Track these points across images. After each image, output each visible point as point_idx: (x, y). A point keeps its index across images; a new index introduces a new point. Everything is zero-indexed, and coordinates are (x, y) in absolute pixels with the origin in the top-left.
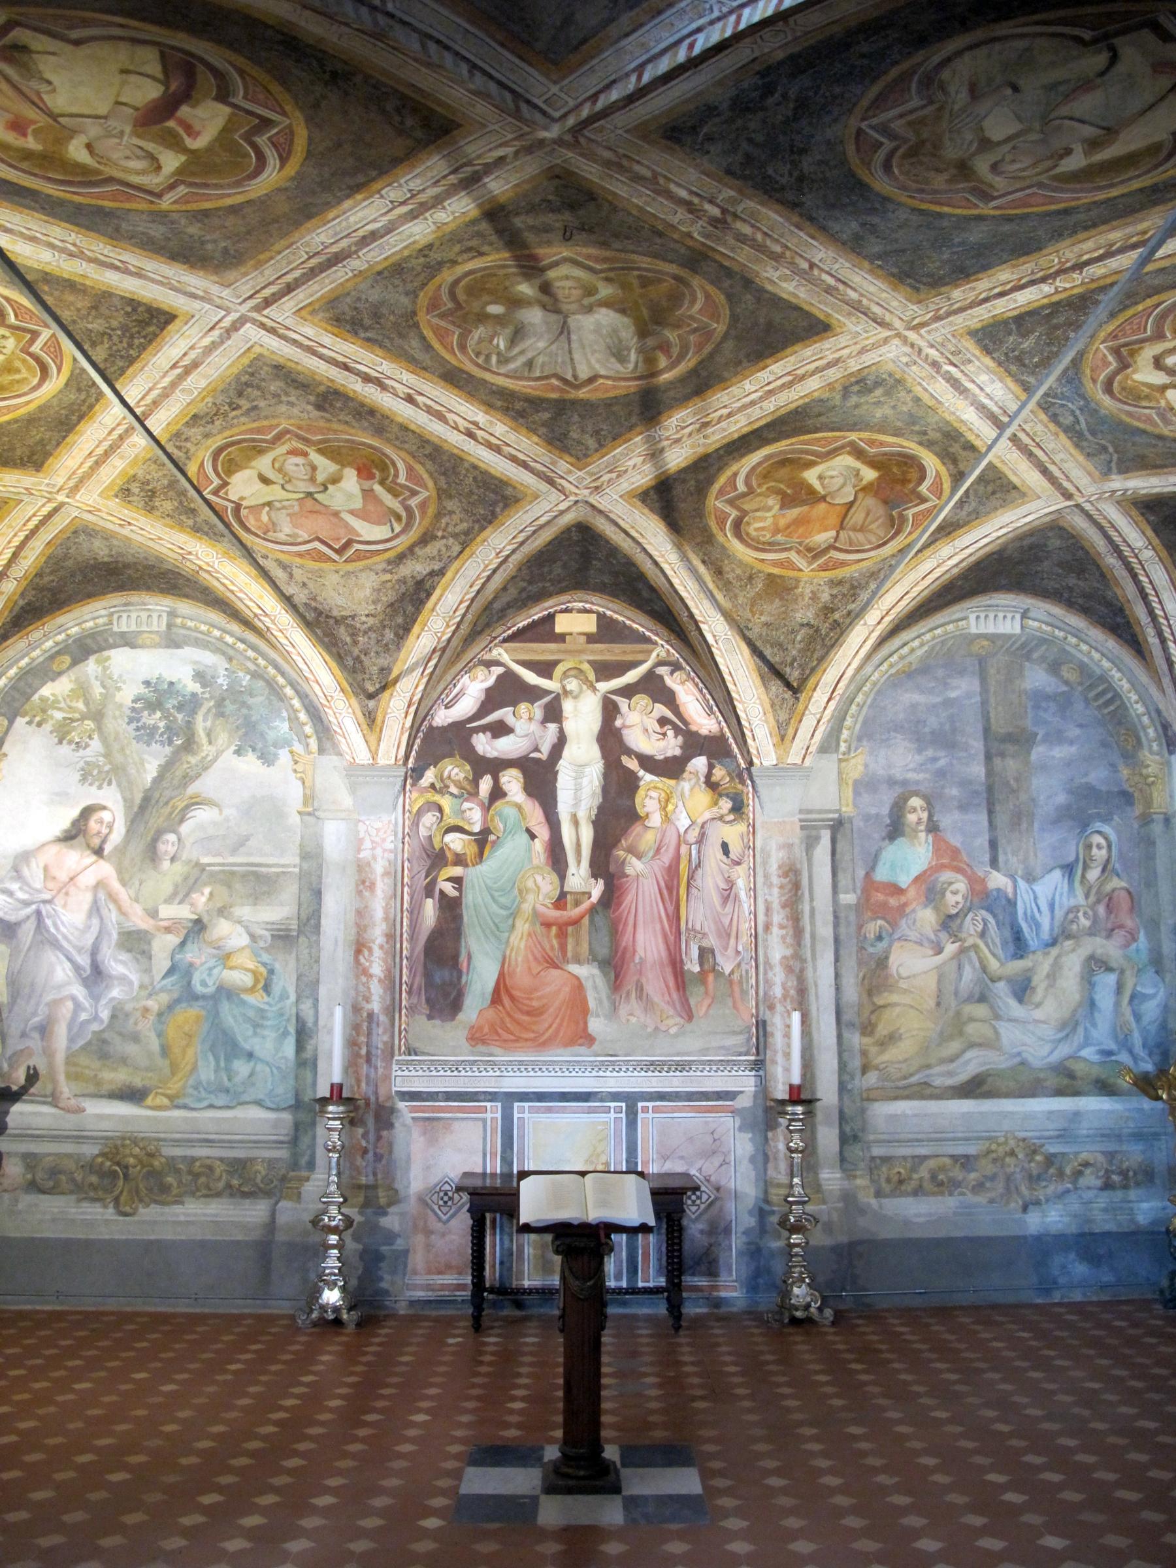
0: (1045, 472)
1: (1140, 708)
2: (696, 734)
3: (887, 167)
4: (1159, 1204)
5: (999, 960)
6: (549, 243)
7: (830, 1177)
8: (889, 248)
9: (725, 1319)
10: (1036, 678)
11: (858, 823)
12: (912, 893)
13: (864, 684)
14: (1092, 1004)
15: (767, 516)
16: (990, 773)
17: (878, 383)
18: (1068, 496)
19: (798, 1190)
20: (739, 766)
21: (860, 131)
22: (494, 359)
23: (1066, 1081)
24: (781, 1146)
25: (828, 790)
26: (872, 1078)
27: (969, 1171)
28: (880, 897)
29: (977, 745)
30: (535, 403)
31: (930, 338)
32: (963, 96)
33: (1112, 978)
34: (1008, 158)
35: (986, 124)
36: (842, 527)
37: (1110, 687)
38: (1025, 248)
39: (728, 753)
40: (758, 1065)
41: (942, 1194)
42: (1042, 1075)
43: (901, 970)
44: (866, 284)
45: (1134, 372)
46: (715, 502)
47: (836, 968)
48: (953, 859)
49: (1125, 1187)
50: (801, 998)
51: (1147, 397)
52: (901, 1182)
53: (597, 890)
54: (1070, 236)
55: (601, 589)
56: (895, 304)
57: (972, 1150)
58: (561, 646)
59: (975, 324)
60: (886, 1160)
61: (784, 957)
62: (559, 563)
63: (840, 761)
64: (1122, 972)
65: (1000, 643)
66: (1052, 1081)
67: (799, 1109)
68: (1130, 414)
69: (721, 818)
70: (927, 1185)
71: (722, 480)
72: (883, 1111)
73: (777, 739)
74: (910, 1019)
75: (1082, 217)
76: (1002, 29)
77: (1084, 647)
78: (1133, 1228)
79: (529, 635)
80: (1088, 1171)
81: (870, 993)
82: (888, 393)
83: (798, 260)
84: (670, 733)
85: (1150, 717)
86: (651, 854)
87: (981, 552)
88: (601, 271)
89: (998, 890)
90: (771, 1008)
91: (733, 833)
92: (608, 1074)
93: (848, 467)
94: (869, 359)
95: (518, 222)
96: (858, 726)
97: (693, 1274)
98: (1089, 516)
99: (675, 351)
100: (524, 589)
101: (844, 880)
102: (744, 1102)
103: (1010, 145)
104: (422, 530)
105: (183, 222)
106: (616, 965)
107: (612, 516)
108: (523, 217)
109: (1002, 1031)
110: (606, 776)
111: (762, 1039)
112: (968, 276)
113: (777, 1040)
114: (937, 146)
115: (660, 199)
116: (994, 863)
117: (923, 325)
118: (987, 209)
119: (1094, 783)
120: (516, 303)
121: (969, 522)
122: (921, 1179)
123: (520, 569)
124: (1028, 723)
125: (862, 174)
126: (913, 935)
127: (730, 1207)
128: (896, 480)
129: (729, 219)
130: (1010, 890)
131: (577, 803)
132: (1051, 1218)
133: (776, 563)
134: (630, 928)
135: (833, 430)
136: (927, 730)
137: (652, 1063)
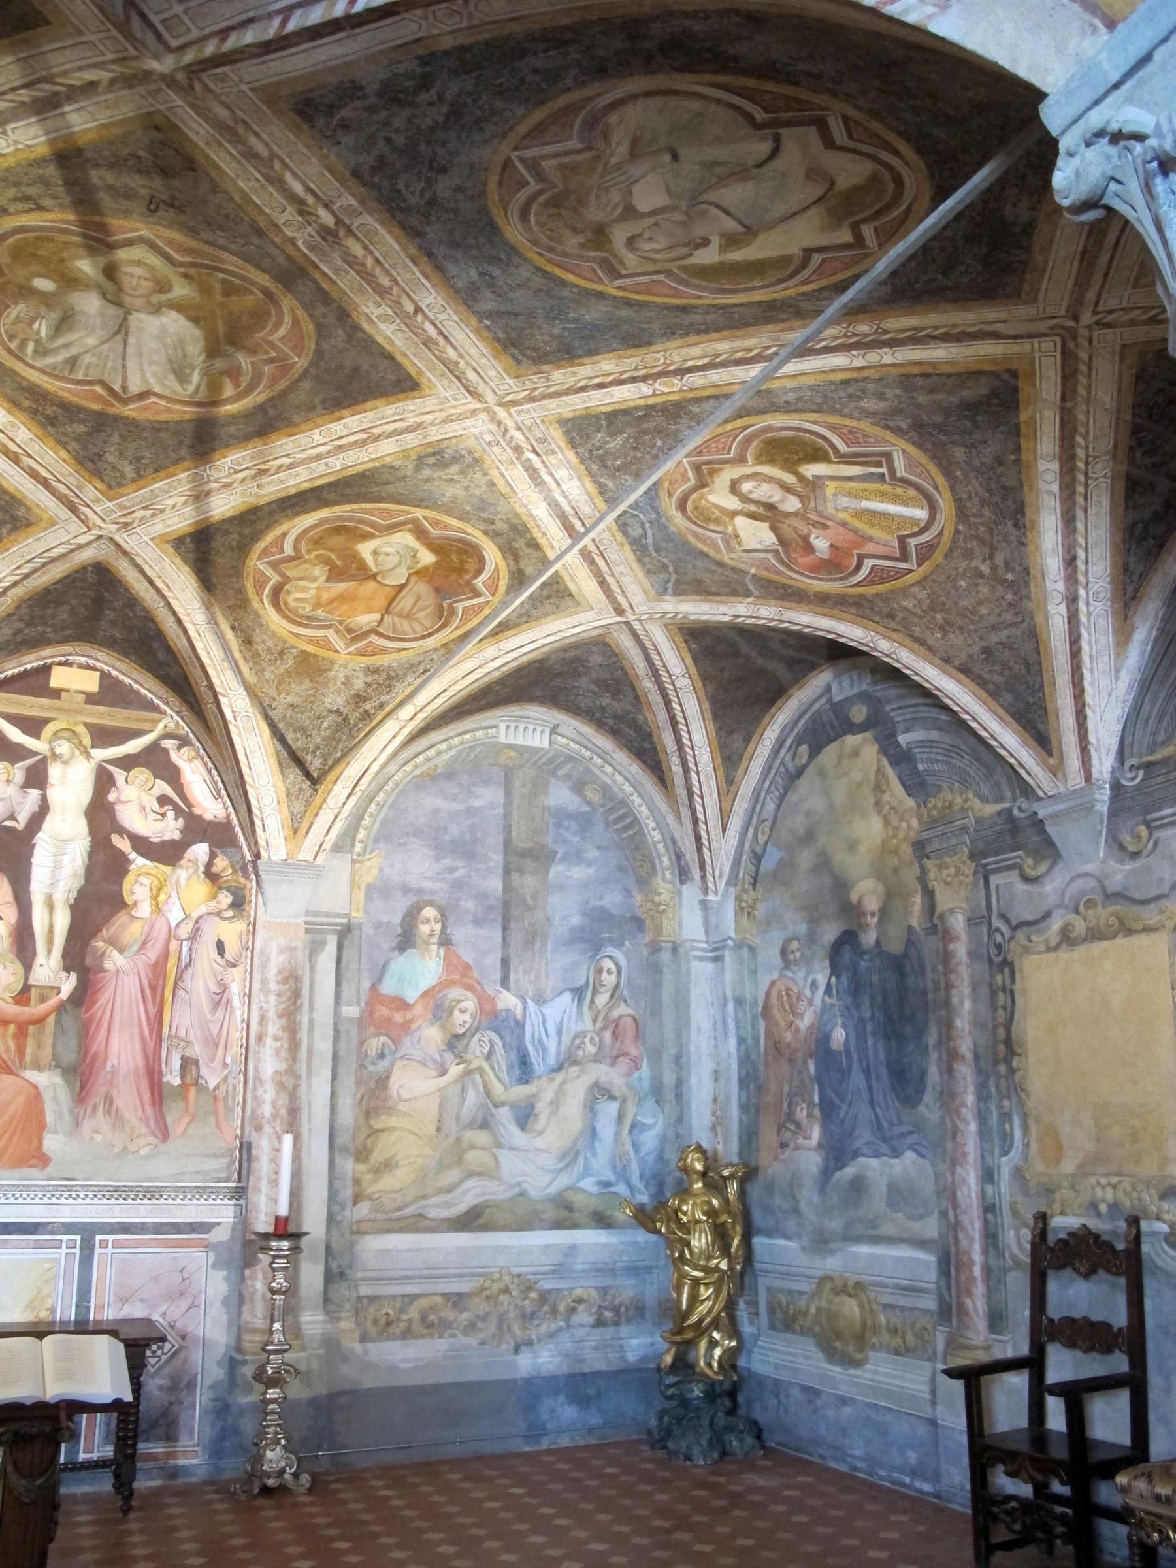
0: (603, 583)
1: (657, 836)
2: (200, 817)
3: (524, 214)
4: (649, 1340)
5: (503, 1084)
6: (127, 213)
7: (312, 1321)
8: (503, 308)
9: (185, 1492)
10: (560, 795)
11: (368, 931)
12: (419, 1009)
13: (385, 783)
14: (594, 1133)
15: (310, 587)
16: (507, 888)
17: (456, 459)
18: (620, 611)
19: (277, 1337)
20: (243, 857)
21: (507, 164)
22: (30, 347)
23: (564, 1213)
24: (259, 1286)
25: (337, 893)
26: (364, 1210)
27: (462, 1311)
28: (385, 1011)
29: (497, 858)
30: (70, 411)
31: (519, 419)
32: (620, 150)
33: (614, 1106)
34: (647, 235)
35: (636, 189)
36: (387, 610)
37: (630, 813)
38: (636, 340)
39: (233, 843)
40: (240, 1193)
41: (431, 1336)
42: (540, 1207)
43: (402, 1092)
44: (469, 344)
45: (710, 492)
46: (256, 563)
47: (332, 1086)
48: (464, 976)
49: (617, 1324)
50: (292, 1119)
51: (717, 521)
52: (388, 1324)
53: (69, 984)
54: (682, 336)
55: (110, 644)
56: (492, 373)
57: (464, 1287)
58: (54, 702)
59: (567, 413)
60: (373, 1299)
61: (276, 1072)
62: (66, 607)
63: (354, 862)
64: (624, 1101)
65: (527, 756)
66: (551, 1214)
67: (285, 1244)
68: (696, 535)
69: (219, 914)
70: (416, 1327)
71: (269, 538)
72: (374, 1245)
73: (289, 832)
74: (408, 1143)
75: (698, 318)
76: (683, 82)
77: (609, 769)
78: (621, 1366)
79: (17, 685)
80: (581, 1308)
81: (367, 1115)
82: (463, 472)
83: (405, 301)
84: (171, 814)
85: (666, 846)
86: (135, 948)
87: (525, 659)
88: (181, 265)
89: (508, 1010)
90: (259, 1128)
91: (231, 931)
92: (63, 1201)
93: (407, 546)
94: (453, 429)
95: (96, 176)
96: (376, 827)
97: (147, 1440)
98: (635, 635)
99: (245, 380)
100: (20, 631)
101: (348, 991)
102: (221, 1235)
103: (652, 220)
106: (82, 1074)
107: (139, 560)
108: (102, 172)
109: (502, 1160)
110: (91, 855)
111: (245, 1164)
112: (573, 358)
113: (263, 1165)
114: (581, 202)
115: (271, 189)
116: (505, 982)
117: (515, 403)
118: (610, 288)
119: (609, 907)
120: (71, 282)
121: (519, 625)
122: (410, 1320)
123: (18, 607)
124: (549, 840)
125: (497, 214)
126: (417, 1054)
127: (196, 1356)
128: (453, 567)
129: (342, 233)
130: (519, 1012)
131: (54, 884)
132: (543, 1359)
133: (313, 641)
134: (103, 1032)
135: (398, 502)
136: (447, 837)
137: (117, 1189)
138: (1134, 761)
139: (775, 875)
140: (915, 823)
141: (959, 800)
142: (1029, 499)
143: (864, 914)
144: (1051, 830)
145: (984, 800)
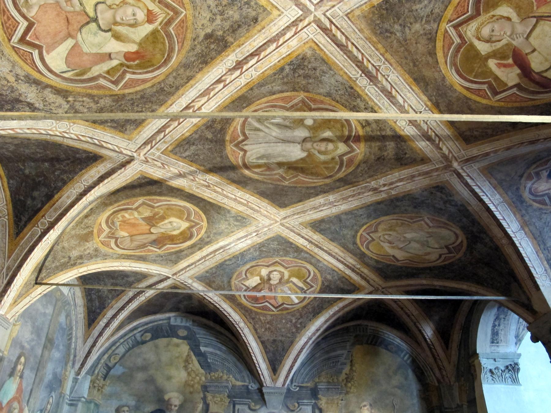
36: (131, 236)
104: (70, 89)
105: (428, 27)
138: (296, 384)
139: (119, 378)
140: (203, 379)
141: (225, 377)
142: (323, 312)
143: (171, 405)
144: (266, 397)
145: (236, 379)
